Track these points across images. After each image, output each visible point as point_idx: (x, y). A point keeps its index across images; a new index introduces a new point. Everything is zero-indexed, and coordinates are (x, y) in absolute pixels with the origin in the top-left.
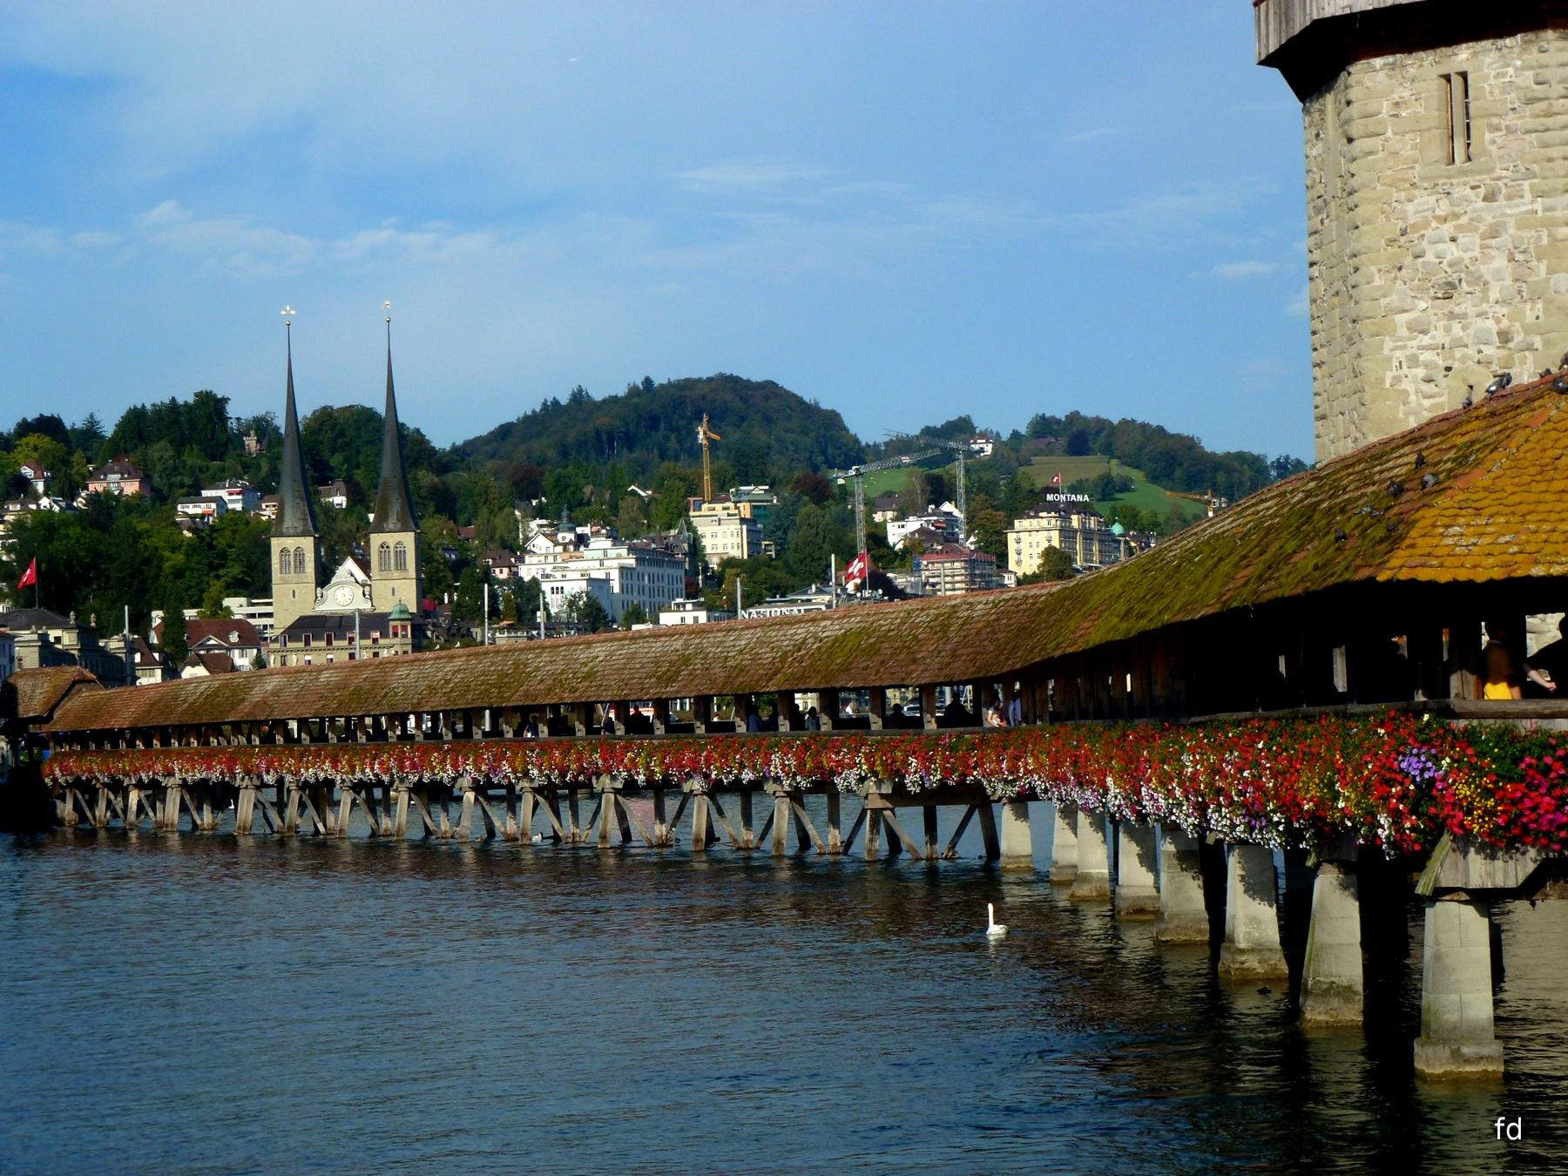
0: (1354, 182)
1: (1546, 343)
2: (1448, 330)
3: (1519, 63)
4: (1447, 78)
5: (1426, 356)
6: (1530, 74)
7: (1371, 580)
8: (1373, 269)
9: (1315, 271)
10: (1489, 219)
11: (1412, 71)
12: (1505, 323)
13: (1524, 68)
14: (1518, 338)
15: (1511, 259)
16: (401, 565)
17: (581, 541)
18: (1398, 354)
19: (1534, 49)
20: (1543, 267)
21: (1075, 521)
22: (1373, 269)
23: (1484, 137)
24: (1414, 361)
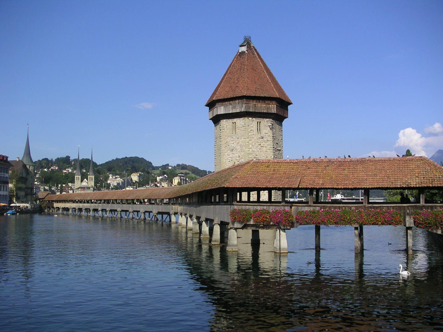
0: (221, 135)
1: (245, 158)
2: (232, 155)
3: (242, 121)
4: (233, 123)
5: (229, 158)
6: (244, 123)
7: (224, 187)
8: (223, 147)
9: (215, 147)
10: (238, 141)
11: (229, 122)
12: (239, 155)
13: (243, 122)
14: (241, 157)
15: (241, 147)
16: (92, 180)
17: (116, 178)
18: (226, 158)
19: (244, 120)
20: (244, 148)
21: (182, 178)
22: (223, 147)
23: (237, 131)
24: (228, 159)
